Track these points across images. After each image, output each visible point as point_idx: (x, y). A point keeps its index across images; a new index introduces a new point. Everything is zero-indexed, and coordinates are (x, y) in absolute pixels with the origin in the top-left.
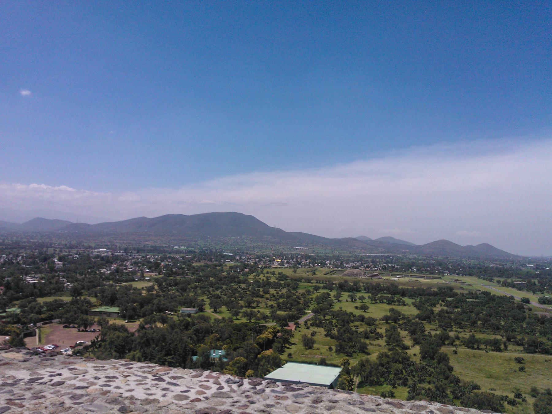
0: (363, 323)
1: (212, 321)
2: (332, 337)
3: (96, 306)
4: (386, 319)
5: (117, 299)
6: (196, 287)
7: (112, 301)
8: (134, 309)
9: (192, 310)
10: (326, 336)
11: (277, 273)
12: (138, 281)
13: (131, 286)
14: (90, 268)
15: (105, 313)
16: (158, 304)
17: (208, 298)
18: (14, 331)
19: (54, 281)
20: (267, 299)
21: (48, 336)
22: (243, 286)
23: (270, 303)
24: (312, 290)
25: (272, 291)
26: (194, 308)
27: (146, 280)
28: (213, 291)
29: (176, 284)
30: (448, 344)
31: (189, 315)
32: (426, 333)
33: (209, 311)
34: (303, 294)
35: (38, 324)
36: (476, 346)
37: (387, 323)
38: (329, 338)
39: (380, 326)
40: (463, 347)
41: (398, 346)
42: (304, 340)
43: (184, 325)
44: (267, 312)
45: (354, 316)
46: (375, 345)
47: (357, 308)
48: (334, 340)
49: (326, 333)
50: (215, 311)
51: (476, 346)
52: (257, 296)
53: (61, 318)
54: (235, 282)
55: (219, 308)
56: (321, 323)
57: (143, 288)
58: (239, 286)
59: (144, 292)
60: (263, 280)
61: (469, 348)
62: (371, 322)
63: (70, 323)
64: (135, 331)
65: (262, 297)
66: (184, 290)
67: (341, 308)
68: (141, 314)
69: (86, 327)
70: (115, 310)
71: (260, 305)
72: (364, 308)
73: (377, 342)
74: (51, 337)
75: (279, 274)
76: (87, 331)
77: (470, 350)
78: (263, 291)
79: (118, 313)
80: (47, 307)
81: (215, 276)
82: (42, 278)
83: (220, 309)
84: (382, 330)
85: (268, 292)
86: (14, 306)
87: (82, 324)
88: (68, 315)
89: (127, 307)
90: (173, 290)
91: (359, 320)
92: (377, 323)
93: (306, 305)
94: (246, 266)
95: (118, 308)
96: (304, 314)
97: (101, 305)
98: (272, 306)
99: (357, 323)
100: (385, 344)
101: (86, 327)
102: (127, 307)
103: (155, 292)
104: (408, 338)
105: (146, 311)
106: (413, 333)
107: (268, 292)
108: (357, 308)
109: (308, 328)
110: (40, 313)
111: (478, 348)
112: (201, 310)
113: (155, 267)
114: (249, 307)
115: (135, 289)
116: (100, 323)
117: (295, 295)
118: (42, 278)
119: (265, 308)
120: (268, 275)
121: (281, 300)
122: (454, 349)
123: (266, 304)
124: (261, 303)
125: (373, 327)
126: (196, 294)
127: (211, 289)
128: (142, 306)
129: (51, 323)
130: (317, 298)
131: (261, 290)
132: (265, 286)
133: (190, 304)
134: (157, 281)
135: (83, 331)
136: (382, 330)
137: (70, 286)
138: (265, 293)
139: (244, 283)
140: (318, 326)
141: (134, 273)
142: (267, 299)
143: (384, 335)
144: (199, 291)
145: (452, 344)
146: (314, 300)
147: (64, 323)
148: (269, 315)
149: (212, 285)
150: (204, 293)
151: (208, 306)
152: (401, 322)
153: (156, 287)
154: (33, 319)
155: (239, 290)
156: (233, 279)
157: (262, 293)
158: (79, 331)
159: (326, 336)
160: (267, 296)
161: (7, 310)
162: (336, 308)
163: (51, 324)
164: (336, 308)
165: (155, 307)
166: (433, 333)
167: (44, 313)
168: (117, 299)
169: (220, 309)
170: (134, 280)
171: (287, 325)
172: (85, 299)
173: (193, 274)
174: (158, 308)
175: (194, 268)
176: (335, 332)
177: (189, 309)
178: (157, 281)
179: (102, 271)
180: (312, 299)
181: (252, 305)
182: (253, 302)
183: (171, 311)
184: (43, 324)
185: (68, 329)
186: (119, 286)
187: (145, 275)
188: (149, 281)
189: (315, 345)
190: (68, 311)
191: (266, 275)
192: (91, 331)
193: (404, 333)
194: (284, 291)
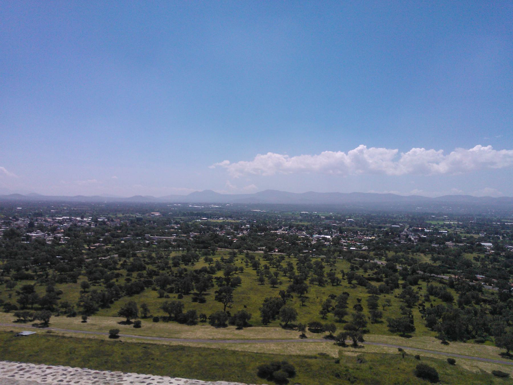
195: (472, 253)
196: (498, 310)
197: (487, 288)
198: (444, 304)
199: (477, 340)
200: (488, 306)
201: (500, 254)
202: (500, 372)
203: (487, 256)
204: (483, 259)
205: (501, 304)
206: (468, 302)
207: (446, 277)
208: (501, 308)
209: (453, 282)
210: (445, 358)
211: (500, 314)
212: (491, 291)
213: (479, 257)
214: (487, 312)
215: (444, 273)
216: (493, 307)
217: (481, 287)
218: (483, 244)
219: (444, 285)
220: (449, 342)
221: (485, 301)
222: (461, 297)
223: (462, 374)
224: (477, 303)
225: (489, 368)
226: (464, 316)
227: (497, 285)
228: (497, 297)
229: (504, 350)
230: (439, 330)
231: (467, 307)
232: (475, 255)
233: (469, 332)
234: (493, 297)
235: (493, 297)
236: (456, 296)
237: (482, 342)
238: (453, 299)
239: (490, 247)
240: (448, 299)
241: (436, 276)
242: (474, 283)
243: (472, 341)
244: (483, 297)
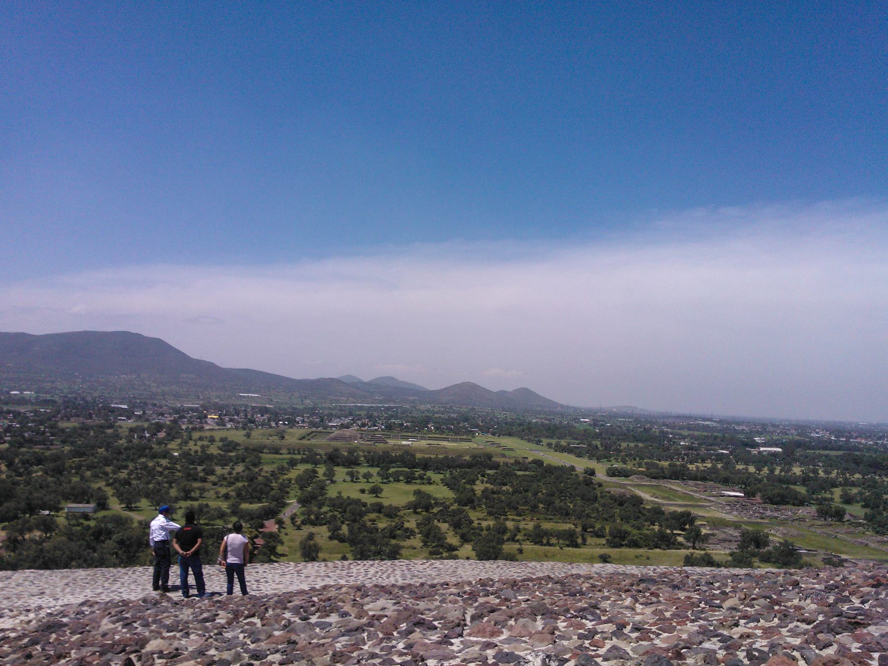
0: (381, 515)
1: (136, 525)
2: (342, 540)
4: (414, 507)
6: (79, 467)
10: (331, 538)
11: (217, 439)
16: (28, 498)
17: (108, 485)
20: (215, 484)
22: (164, 462)
23: (223, 491)
24: (286, 466)
25: (219, 470)
26: (88, 502)
28: (114, 473)
29: (40, 461)
30: (508, 540)
31: (86, 517)
32: (475, 524)
33: (116, 507)
34: (273, 474)
36: (545, 541)
37: (415, 513)
38: (336, 542)
39: (407, 518)
40: (528, 542)
41: (442, 546)
42: (304, 548)
43: (93, 534)
44: (224, 506)
45: (365, 505)
46: (408, 548)
47: (363, 491)
48: (346, 544)
49: (329, 534)
50: (127, 507)
51: (545, 541)
52: (196, 480)
54: (146, 456)
56: (317, 518)
58: (157, 463)
60: (196, 452)
61: (536, 543)
62: (391, 513)
65: (204, 480)
66: (59, 471)
67: (339, 493)
71: (206, 494)
72: (376, 491)
73: (408, 543)
75: (222, 440)
77: (537, 547)
78: (203, 470)
81: (108, 446)
83: (138, 504)
84: (411, 523)
85: (212, 473)
90: (37, 473)
91: (374, 511)
92: (401, 513)
93: (284, 490)
94: (159, 427)
96: (285, 505)
98: (226, 497)
99: (373, 516)
100: (421, 544)
104: (451, 533)
106: (456, 526)
107: (212, 473)
108: (363, 491)
109: (299, 528)
111: (549, 544)
112: (102, 505)
114: (187, 497)
117: (260, 475)
119: (214, 500)
120: (206, 443)
121: (240, 485)
122: (517, 546)
123: (217, 493)
124: (208, 491)
125: (396, 520)
126: (82, 478)
127: (109, 469)
130: (299, 479)
131: (200, 468)
132: (203, 462)
133: (81, 496)
136: (411, 523)
138: (207, 474)
139: (164, 457)
140: (314, 524)
142: (215, 484)
143: (417, 531)
144: (88, 473)
145: (513, 539)
146: (293, 482)
148: (228, 511)
149: (107, 462)
150: (96, 476)
152: (435, 510)
155: (159, 469)
156: (143, 450)
157: (201, 474)
159: (331, 538)
160: (212, 478)
162: (332, 492)
164: (332, 492)
165: (23, 505)
166: (484, 524)
169: (138, 504)
171: (263, 526)
173: (64, 442)
175: (63, 431)
176: (345, 530)
177: (81, 505)
180: (290, 480)
181: (193, 494)
182: (193, 490)
183: (50, 510)
189: (321, 555)
191: (200, 443)
193: (444, 527)
194: (240, 468)
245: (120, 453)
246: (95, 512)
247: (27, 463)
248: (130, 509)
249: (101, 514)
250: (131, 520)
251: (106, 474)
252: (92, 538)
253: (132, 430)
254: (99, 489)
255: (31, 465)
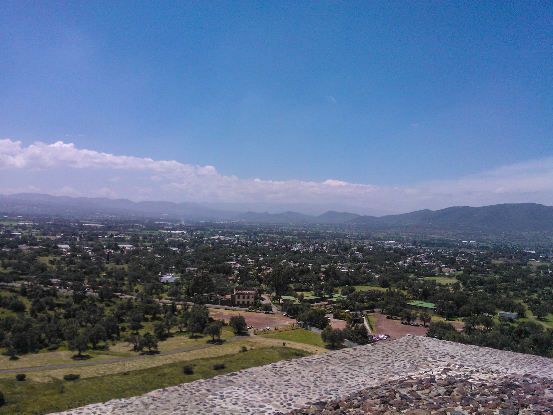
1: (545, 331)
3: (408, 299)
5: (429, 295)
6: (505, 289)
7: (425, 297)
8: (451, 307)
9: (514, 315)
12: (438, 276)
13: (435, 281)
14: (388, 260)
15: (421, 308)
17: (525, 302)
18: (348, 317)
19: (362, 271)
21: (376, 326)
26: (512, 312)
27: (446, 276)
28: (529, 295)
29: (482, 283)
31: (512, 321)
33: (531, 317)
35: (365, 312)
43: (516, 332)
50: (538, 318)
53: (383, 308)
55: (544, 316)
57: (447, 284)
59: (451, 288)
63: (392, 315)
64: (462, 331)
66: (493, 290)
68: (460, 313)
69: (409, 321)
70: (431, 306)
74: (380, 326)
76: (410, 324)
79: (435, 309)
80: (368, 296)
81: (524, 277)
82: (350, 267)
83: (546, 317)
86: (337, 292)
87: (405, 317)
88: (390, 307)
89: (444, 304)
90: (481, 290)
95: (434, 305)
97: (414, 299)
101: (409, 321)
102: (444, 304)
103: (461, 290)
105: (465, 311)
110: (362, 301)
112: (522, 314)
113: (451, 263)
115: (440, 285)
116: (422, 318)
118: (350, 267)
126: (508, 296)
127: (525, 292)
128: (459, 305)
129: (374, 312)
133: (508, 307)
134: (459, 278)
135: (406, 324)
137: (377, 276)
141: (432, 267)
144: (512, 293)
147: (387, 314)
151: (530, 312)
153: (461, 285)
154: (360, 307)
158: (403, 323)
161: (333, 296)
163: (375, 314)
165: (473, 308)
167: (366, 302)
168: (429, 295)
169: (546, 317)
170: (434, 275)
172: (398, 292)
173: (495, 272)
174: (477, 308)
175: (494, 265)
177: (508, 313)
178: (459, 278)
179: (400, 263)
184: (368, 312)
185: (391, 320)
186: (423, 280)
187: (443, 270)
188: (450, 277)
190: (387, 303)
192: (414, 325)
195: (47, 256)
196: (72, 313)
197: (63, 291)
198: (15, 315)
199: (50, 347)
200: (63, 311)
201: (76, 256)
202: (71, 375)
203: (64, 259)
204: (59, 262)
205: (75, 306)
206: (41, 309)
207: (18, 285)
208: (75, 310)
209: (25, 289)
210: (13, 375)
211: (74, 316)
212: (65, 294)
213: (55, 260)
214: (61, 317)
215: (15, 280)
216: (67, 311)
217: (55, 291)
218: (59, 246)
219: (15, 294)
220: (19, 356)
221: (59, 306)
222: (33, 305)
223: (32, 388)
224: (51, 309)
225: (60, 374)
226: (37, 325)
227: (72, 288)
228: (72, 300)
229: (76, 353)
230: (7, 345)
231: (40, 315)
232: (51, 258)
233: (41, 341)
234: (68, 300)
235: (68, 300)
236: (28, 304)
237: (55, 349)
238: (25, 308)
239: (66, 249)
240: (19, 308)
241: (5, 284)
242: (49, 288)
243: (45, 349)
244: (57, 302)
245: (532, 282)
246: (517, 318)
247: (473, 283)
248: (541, 320)
249: (521, 320)
250: (542, 327)
251: (523, 295)
252: (516, 334)
253: (539, 268)
254: (519, 304)
255: (477, 285)
